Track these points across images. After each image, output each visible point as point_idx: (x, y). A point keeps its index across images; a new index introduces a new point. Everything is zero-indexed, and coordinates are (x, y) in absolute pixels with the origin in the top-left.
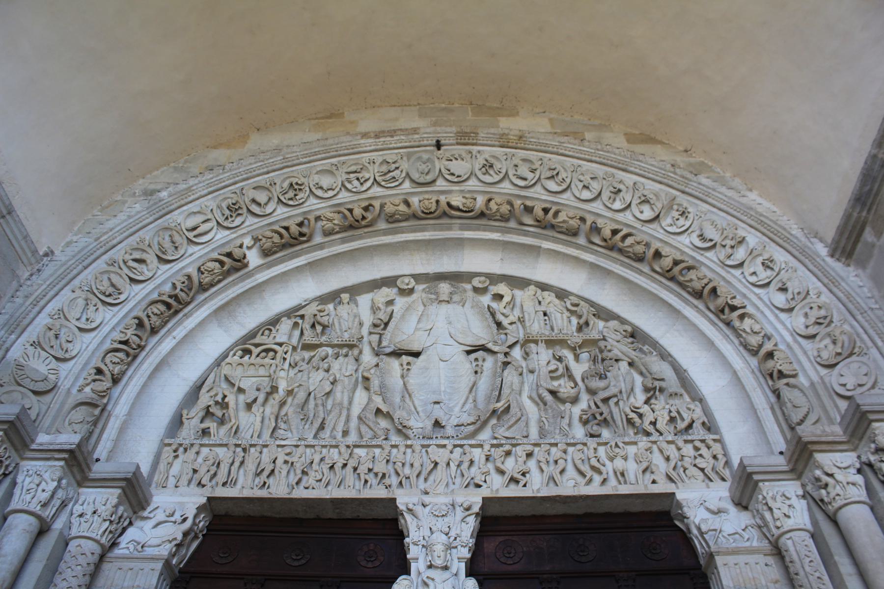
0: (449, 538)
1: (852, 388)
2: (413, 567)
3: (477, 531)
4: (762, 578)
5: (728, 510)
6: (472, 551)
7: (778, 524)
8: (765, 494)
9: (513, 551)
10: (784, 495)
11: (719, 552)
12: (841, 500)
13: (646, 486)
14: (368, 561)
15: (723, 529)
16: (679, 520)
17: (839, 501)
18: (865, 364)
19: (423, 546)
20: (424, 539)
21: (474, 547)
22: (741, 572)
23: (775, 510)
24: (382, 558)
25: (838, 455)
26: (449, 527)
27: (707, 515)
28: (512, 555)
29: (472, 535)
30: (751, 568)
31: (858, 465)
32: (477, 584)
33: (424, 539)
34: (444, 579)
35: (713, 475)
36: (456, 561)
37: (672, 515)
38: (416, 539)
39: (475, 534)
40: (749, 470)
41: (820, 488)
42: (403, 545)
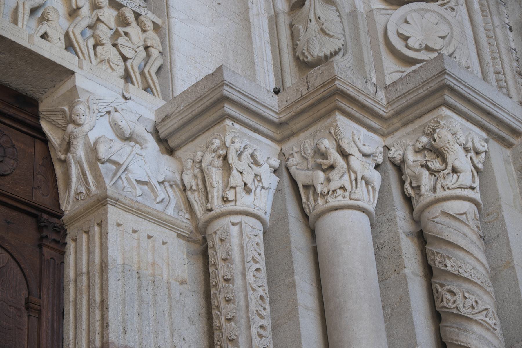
1: (417, 46)
4: (165, 267)
5: (146, 141)
7: (230, 195)
8: (228, 142)
10: (252, 156)
11: (117, 200)
12: (344, 197)
13: (31, 36)
15: (130, 167)
16: (50, 122)
17: (340, 198)
18: (448, 23)
22: (139, 246)
23: (234, 172)
25: (364, 131)
27: (110, 134)
30: (154, 247)
31: (380, 159)
35: (136, 76)
37: (42, 108)
40: (227, 91)
41: (319, 167)
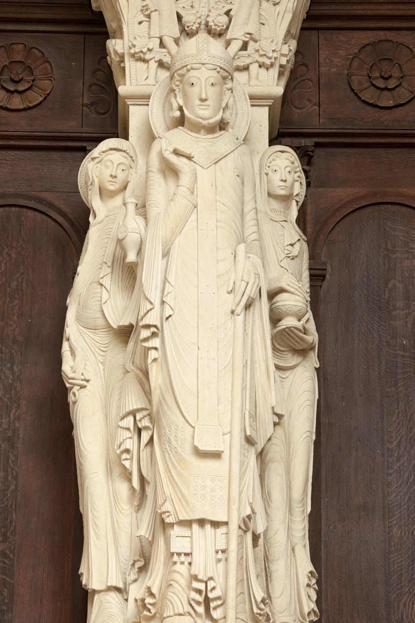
0: (228, 43)
2: (136, 116)
3: (302, 15)
6: (287, 74)
9: (397, 73)
14: (12, 92)
19: (161, 64)
20: (162, 45)
21: (293, 58)
24: (47, 84)
26: (228, 13)
28: (392, 84)
29: (288, 31)
32: (298, 163)
33: (162, 45)
34: (215, 157)
36: (244, 104)
38: (141, 44)
39: (296, 30)
42: (104, 53)
